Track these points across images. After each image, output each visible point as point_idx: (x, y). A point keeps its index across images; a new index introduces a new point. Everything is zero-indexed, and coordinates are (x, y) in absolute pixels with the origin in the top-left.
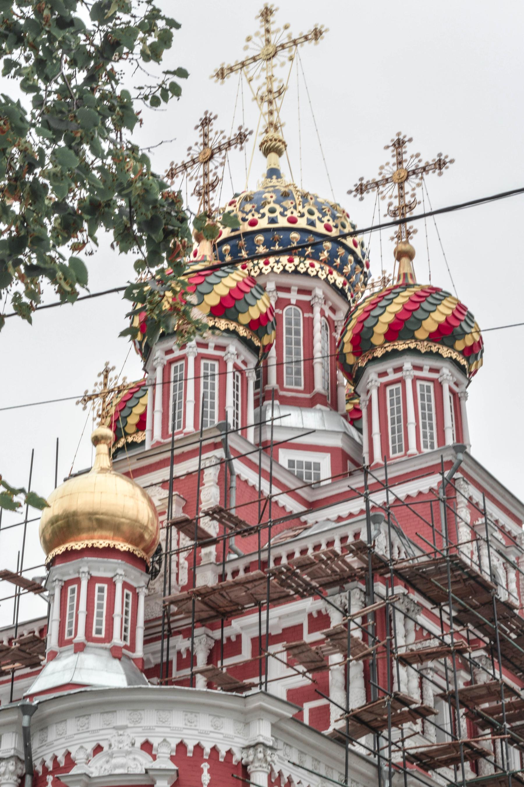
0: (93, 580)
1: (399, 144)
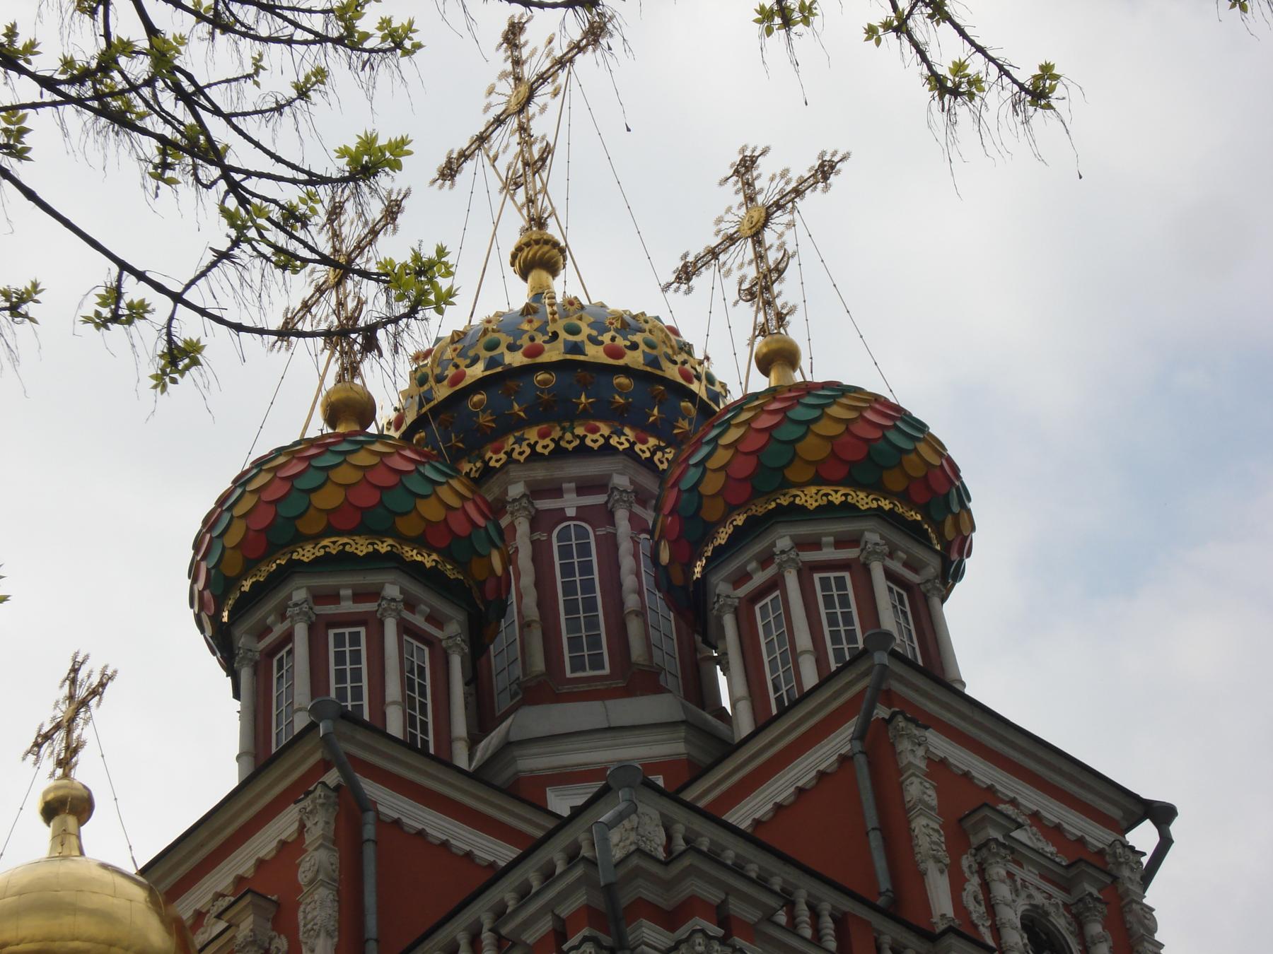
1: (746, 166)
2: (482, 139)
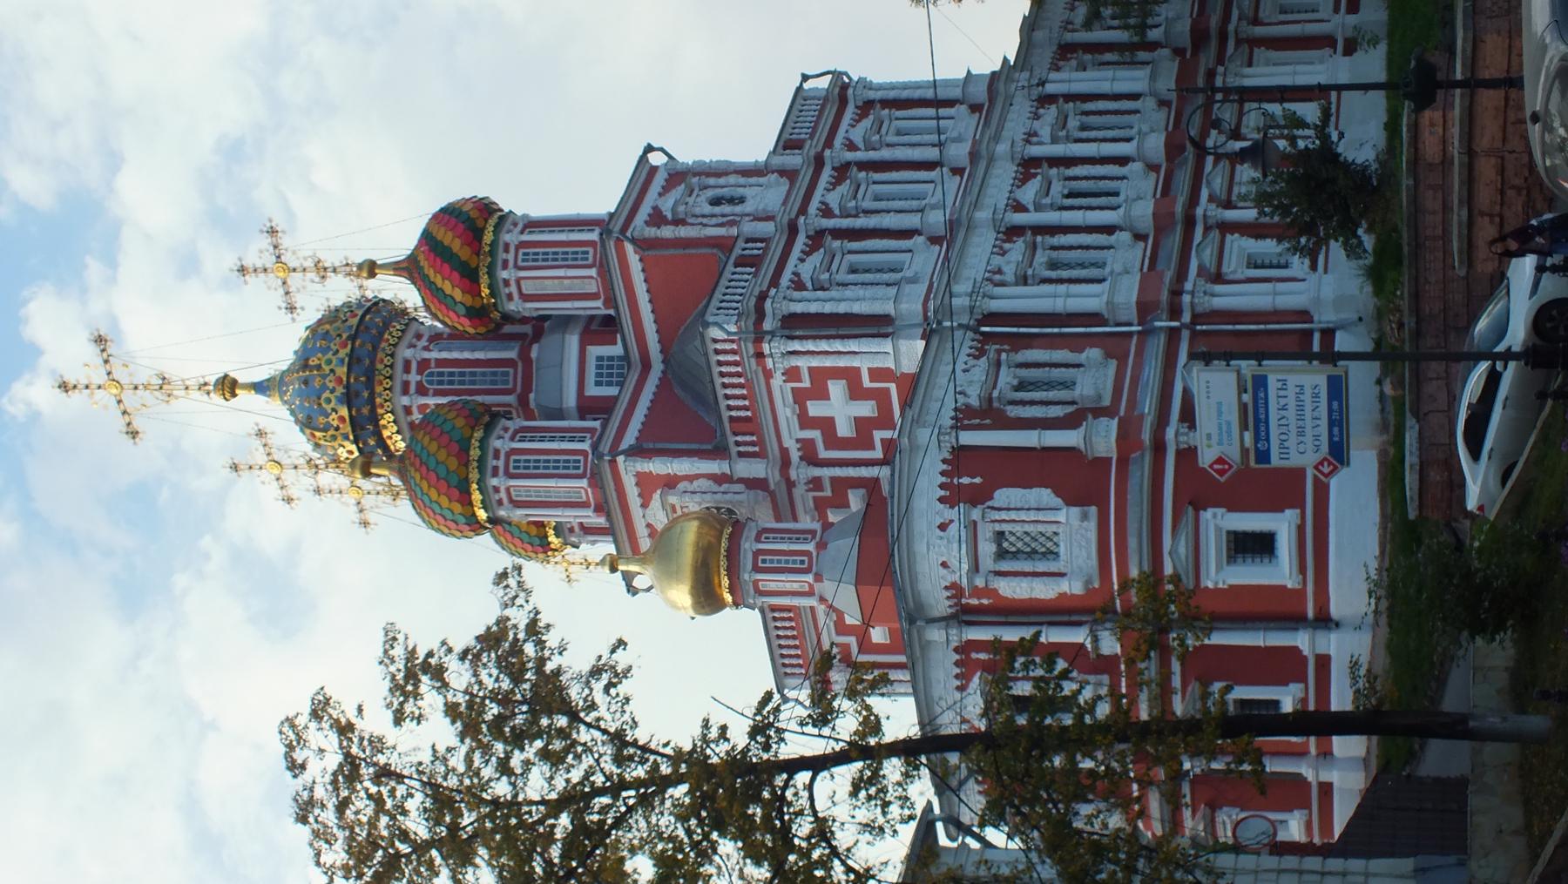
0: (756, 569)
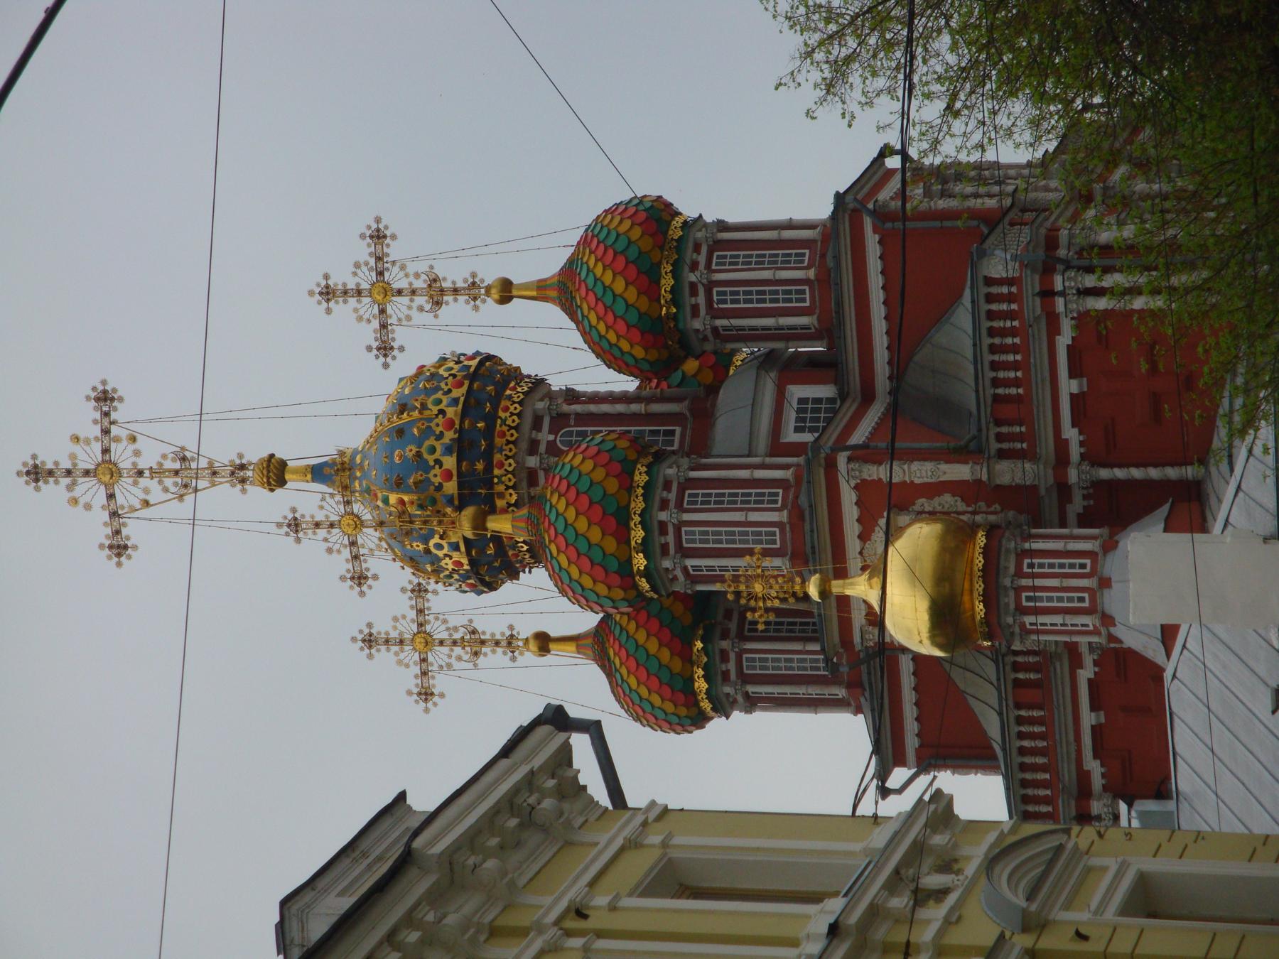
1: (328, 293)
2: (114, 514)
